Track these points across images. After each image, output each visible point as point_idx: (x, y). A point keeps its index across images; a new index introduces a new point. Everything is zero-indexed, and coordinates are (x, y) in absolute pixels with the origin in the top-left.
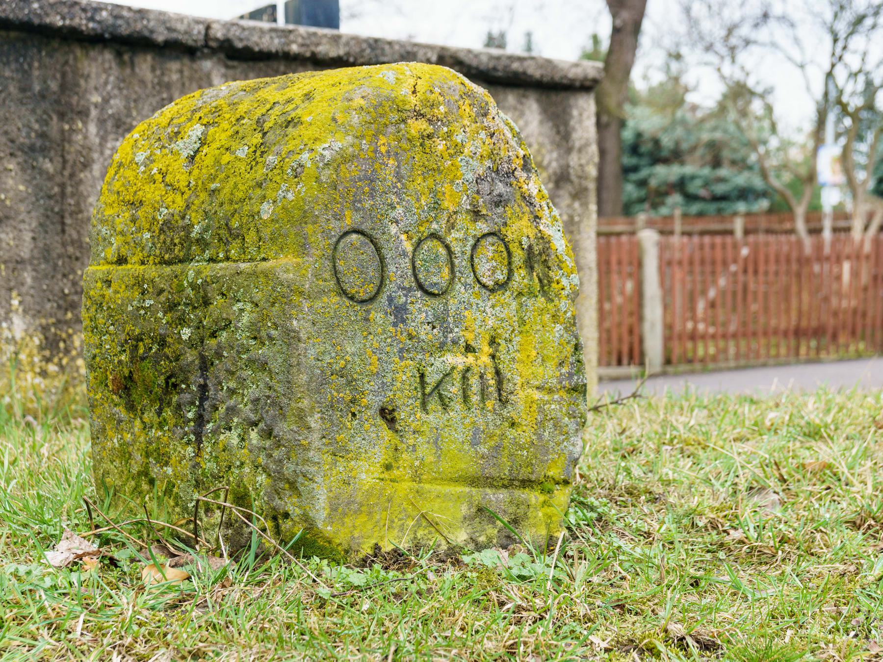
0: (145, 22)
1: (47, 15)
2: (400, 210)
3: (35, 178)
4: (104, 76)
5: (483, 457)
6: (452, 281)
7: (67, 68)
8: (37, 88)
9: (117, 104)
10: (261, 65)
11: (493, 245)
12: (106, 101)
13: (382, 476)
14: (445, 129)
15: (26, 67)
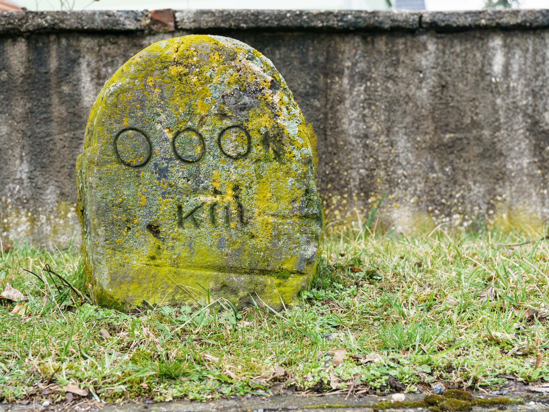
0: (376, 18)
1: (312, 21)
2: (163, 116)
3: (308, 110)
4: (354, 51)
5: (227, 255)
6: (203, 154)
7: (331, 49)
8: (311, 61)
9: (362, 66)
10: (462, 34)
11: (236, 132)
12: (355, 64)
13: (148, 263)
14: (198, 70)
15: (304, 50)
